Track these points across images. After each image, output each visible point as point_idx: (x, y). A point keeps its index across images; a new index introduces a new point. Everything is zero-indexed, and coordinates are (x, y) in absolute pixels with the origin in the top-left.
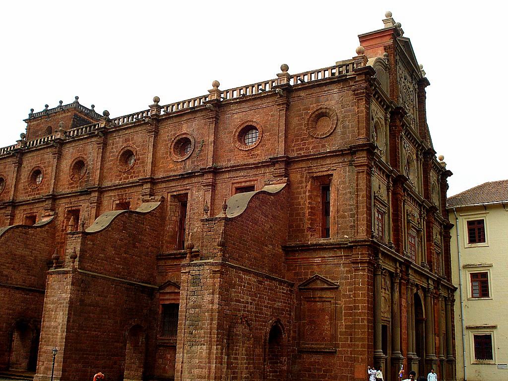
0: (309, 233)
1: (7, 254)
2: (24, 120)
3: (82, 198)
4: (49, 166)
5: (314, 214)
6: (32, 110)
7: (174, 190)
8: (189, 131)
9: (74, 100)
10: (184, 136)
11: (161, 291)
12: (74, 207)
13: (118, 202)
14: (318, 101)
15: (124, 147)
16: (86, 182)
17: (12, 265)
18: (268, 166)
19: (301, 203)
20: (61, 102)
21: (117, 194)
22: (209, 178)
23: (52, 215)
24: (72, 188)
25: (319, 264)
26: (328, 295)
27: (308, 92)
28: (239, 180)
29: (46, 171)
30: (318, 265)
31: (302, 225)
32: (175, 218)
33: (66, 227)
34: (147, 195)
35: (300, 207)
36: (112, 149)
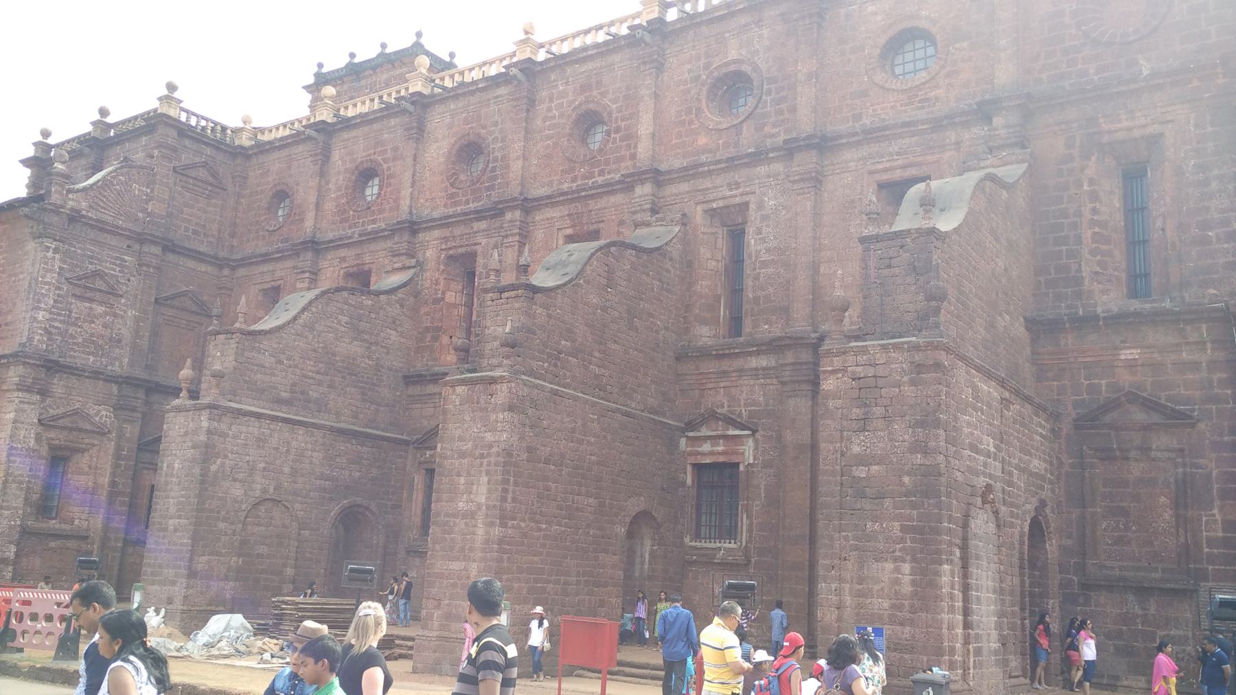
0: (1096, 287)
1: (315, 351)
2: (304, 87)
3: (483, 225)
4: (395, 159)
6: (320, 66)
7: (711, 197)
9: (414, 39)
10: (732, 68)
11: (691, 434)
13: (569, 231)
15: (580, 104)
16: (488, 189)
17: (329, 378)
20: (384, 46)
21: (567, 213)
22: (806, 161)
23: (409, 268)
24: (456, 204)
28: (888, 165)
29: (389, 168)
30: (1131, 365)
31: (1074, 267)
32: (714, 263)
33: (443, 293)
34: (644, 210)
36: (549, 109)
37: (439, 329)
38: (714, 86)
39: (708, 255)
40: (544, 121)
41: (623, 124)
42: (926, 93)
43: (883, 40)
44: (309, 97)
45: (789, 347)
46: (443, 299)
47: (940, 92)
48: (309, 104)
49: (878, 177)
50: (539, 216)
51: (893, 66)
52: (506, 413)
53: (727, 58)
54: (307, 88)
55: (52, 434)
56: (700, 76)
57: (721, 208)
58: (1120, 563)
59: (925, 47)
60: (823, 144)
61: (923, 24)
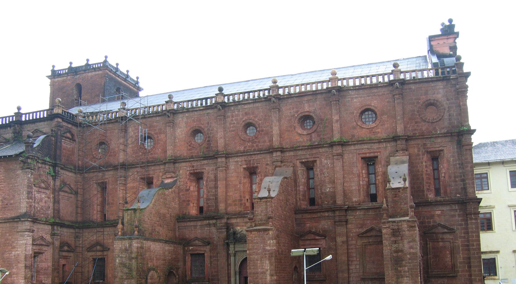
2: (47, 77)
3: (205, 162)
4: (160, 133)
5: (429, 179)
6: (54, 67)
7: (303, 157)
8: (312, 109)
9: (104, 59)
10: (307, 114)
11: (303, 238)
12: (196, 170)
13: (245, 166)
14: (426, 94)
18: (389, 142)
19: (420, 170)
21: (244, 159)
22: (338, 150)
23: (174, 177)
25: (439, 215)
26: (448, 236)
27: (417, 86)
32: (303, 180)
35: (419, 173)
37: (189, 201)
38: (300, 119)
39: (302, 177)
40: (230, 124)
41: (264, 129)
42: (375, 130)
43: (360, 111)
44: (49, 80)
45: (337, 210)
46: (190, 189)
47: (379, 130)
48: (50, 84)
49: (361, 155)
50: (231, 160)
51: (362, 119)
52: (274, 241)
53: (304, 110)
54: (48, 77)
55: (34, 248)
56: (294, 115)
57: (306, 162)
58: (437, 270)
59: (372, 114)
60: (343, 144)
61: (372, 108)
